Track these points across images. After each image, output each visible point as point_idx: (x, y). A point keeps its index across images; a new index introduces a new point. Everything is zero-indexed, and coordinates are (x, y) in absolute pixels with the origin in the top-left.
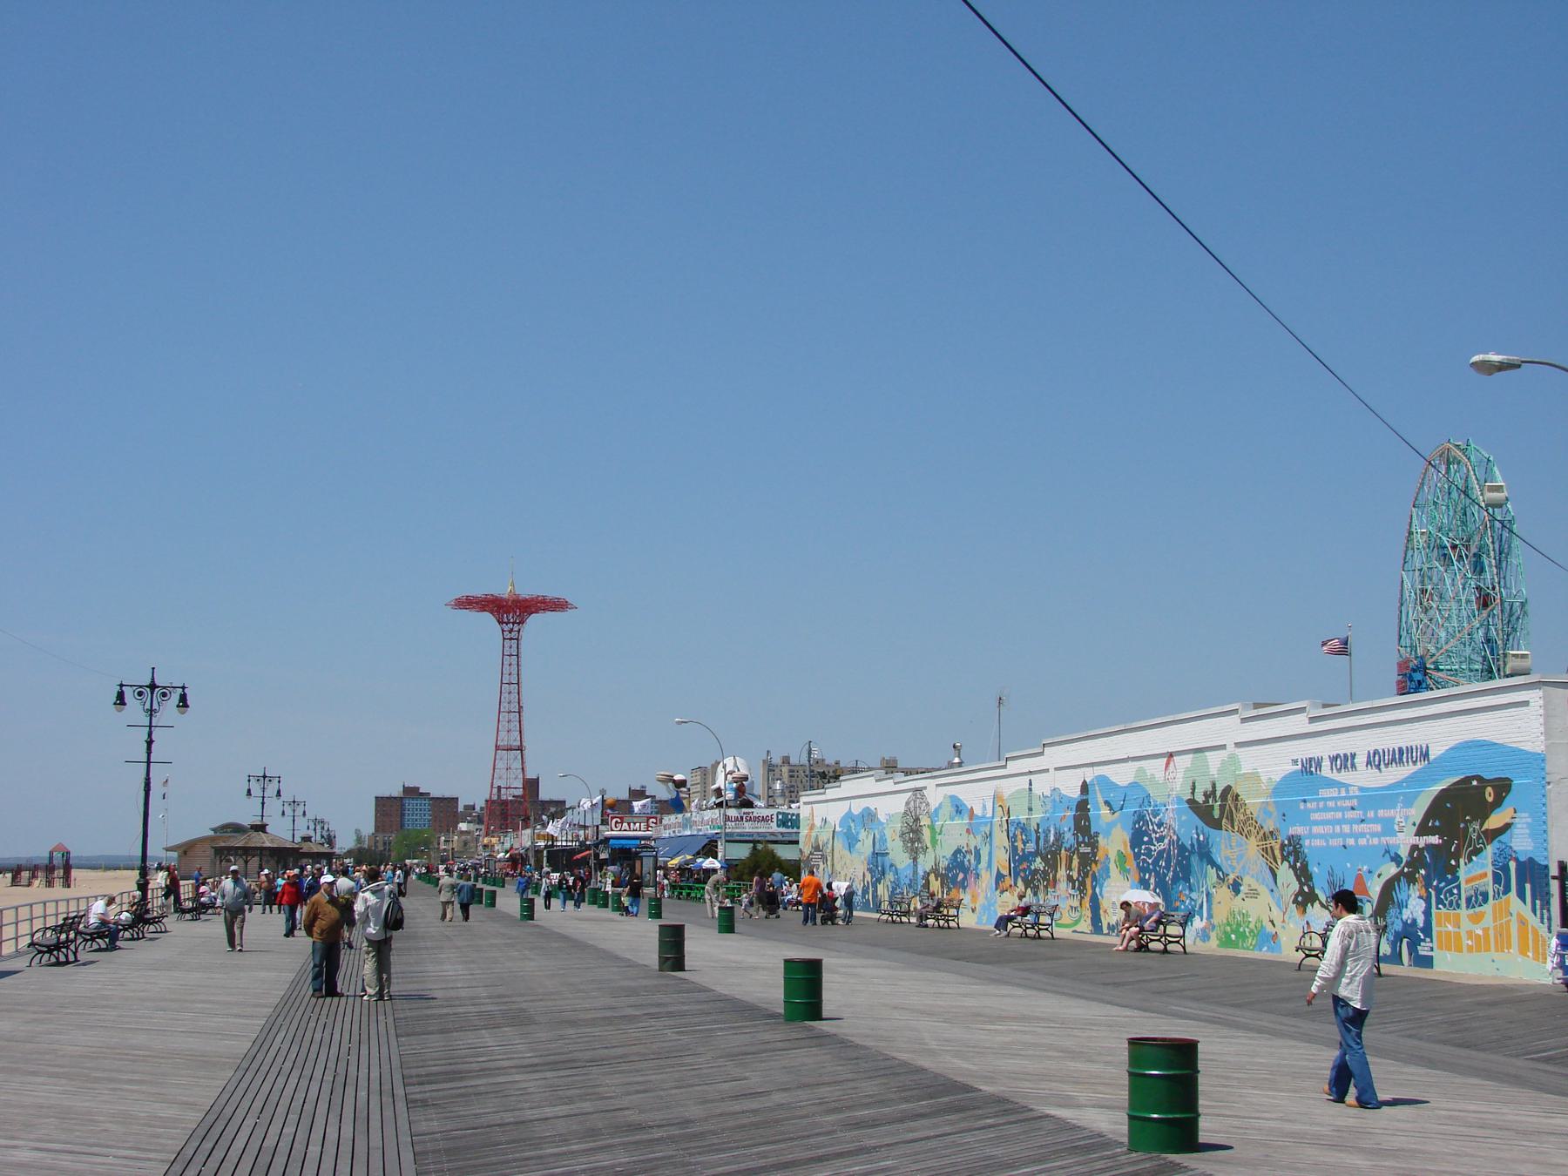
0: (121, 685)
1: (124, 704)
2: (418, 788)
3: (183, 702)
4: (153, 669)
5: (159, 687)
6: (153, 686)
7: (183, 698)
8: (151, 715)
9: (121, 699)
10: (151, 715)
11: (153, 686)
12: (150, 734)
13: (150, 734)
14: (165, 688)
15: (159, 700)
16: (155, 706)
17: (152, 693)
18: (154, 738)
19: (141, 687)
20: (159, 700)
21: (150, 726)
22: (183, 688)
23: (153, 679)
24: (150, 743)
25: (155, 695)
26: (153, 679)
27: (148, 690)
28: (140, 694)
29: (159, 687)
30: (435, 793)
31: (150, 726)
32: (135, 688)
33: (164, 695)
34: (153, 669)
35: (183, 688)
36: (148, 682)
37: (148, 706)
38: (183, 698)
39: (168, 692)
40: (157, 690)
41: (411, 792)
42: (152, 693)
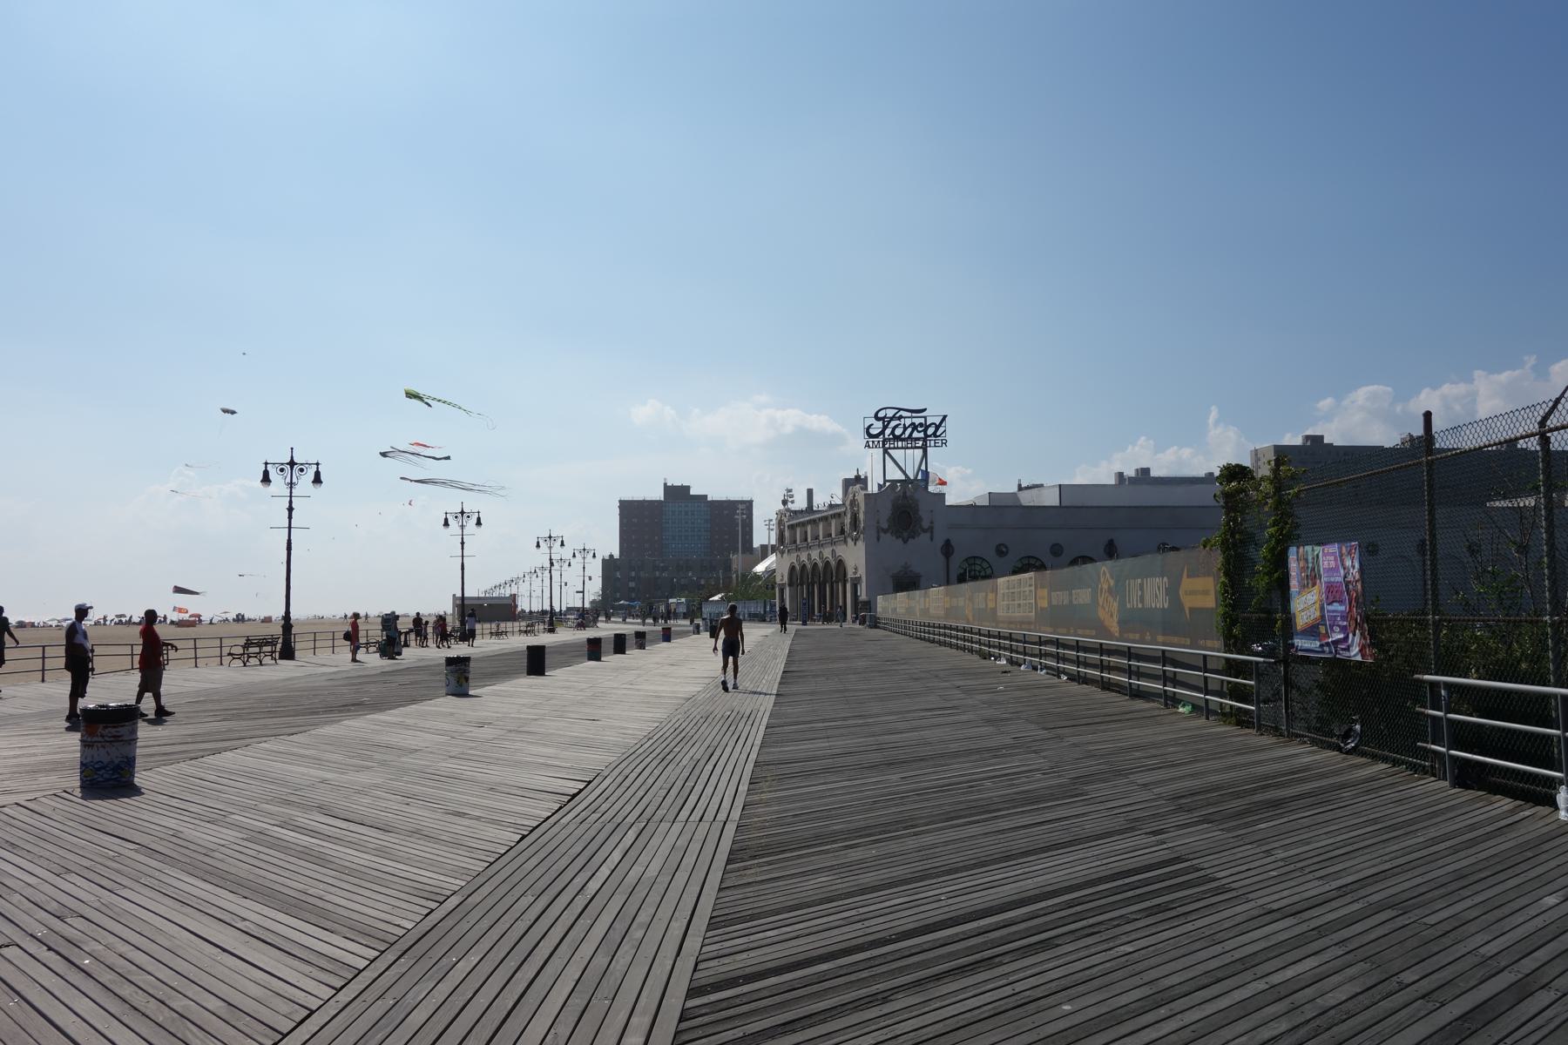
0: (266, 464)
1: (270, 481)
2: (688, 488)
4: (292, 449)
6: (292, 463)
8: (291, 488)
9: (266, 479)
10: (291, 488)
12: (291, 502)
14: (302, 464)
18: (293, 506)
19: (282, 464)
21: (291, 497)
22: (318, 464)
23: (292, 457)
26: (292, 457)
27: (288, 466)
28: (282, 470)
29: (297, 464)
30: (715, 494)
31: (291, 497)
33: (302, 470)
35: (318, 464)
36: (288, 460)
37: (288, 480)
40: (295, 466)
41: (677, 493)
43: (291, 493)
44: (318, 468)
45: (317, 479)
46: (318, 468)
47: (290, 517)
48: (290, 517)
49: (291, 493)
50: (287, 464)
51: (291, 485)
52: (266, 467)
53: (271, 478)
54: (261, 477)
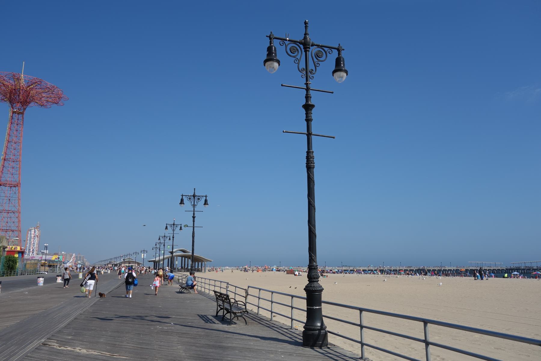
3: (206, 203)
4: (195, 189)
5: (196, 196)
6: (194, 196)
7: (206, 201)
8: (194, 207)
9: (182, 202)
11: (194, 196)
12: (194, 214)
13: (194, 214)
14: (199, 196)
15: (197, 201)
17: (194, 199)
18: (195, 215)
21: (194, 211)
22: (206, 196)
24: (194, 217)
25: (195, 200)
27: (193, 197)
28: (190, 199)
29: (196, 196)
31: (194, 211)
32: (188, 196)
33: (199, 199)
34: (195, 189)
35: (206, 196)
36: (192, 194)
37: (193, 203)
38: (206, 201)
39: (200, 198)
40: (196, 197)
42: (194, 199)
43: (194, 209)
45: (206, 203)
47: (194, 221)
48: (194, 221)
49: (194, 209)
51: (194, 206)
52: (182, 197)
53: (184, 202)
54: (180, 202)
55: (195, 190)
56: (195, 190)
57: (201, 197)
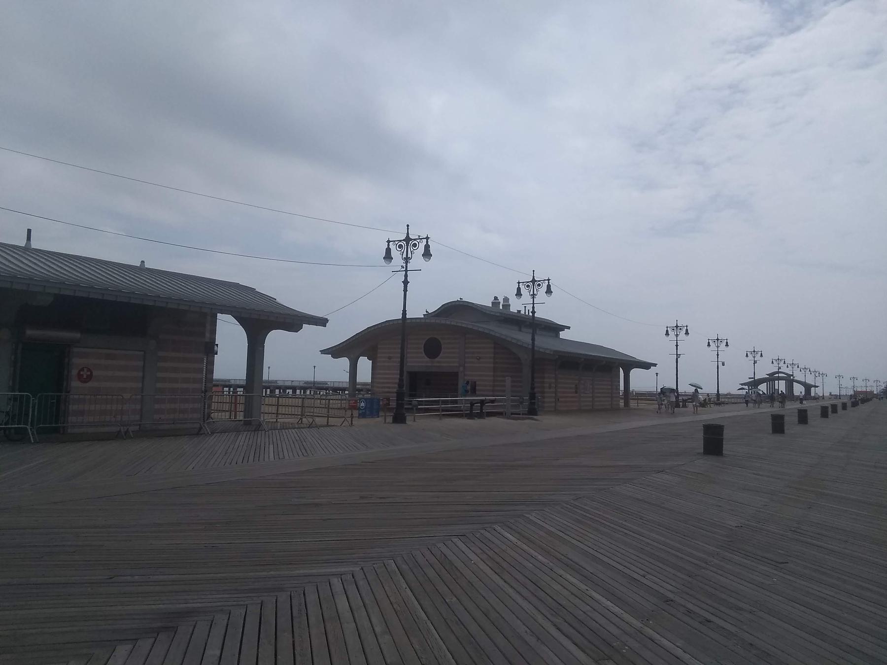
0: (389, 242)
4: (408, 226)
11: (408, 239)
12: (406, 276)
13: (406, 276)
14: (415, 240)
15: (412, 250)
16: (409, 255)
20: (412, 250)
22: (427, 238)
23: (408, 234)
24: (406, 283)
26: (408, 234)
27: (405, 242)
28: (400, 246)
29: (411, 239)
31: (406, 271)
32: (397, 242)
34: (408, 226)
35: (427, 238)
37: (405, 256)
40: (411, 242)
44: (427, 242)
46: (427, 242)
47: (405, 290)
48: (405, 290)
50: (404, 240)
52: (388, 245)
55: (408, 229)
56: (408, 229)
57: (418, 241)
